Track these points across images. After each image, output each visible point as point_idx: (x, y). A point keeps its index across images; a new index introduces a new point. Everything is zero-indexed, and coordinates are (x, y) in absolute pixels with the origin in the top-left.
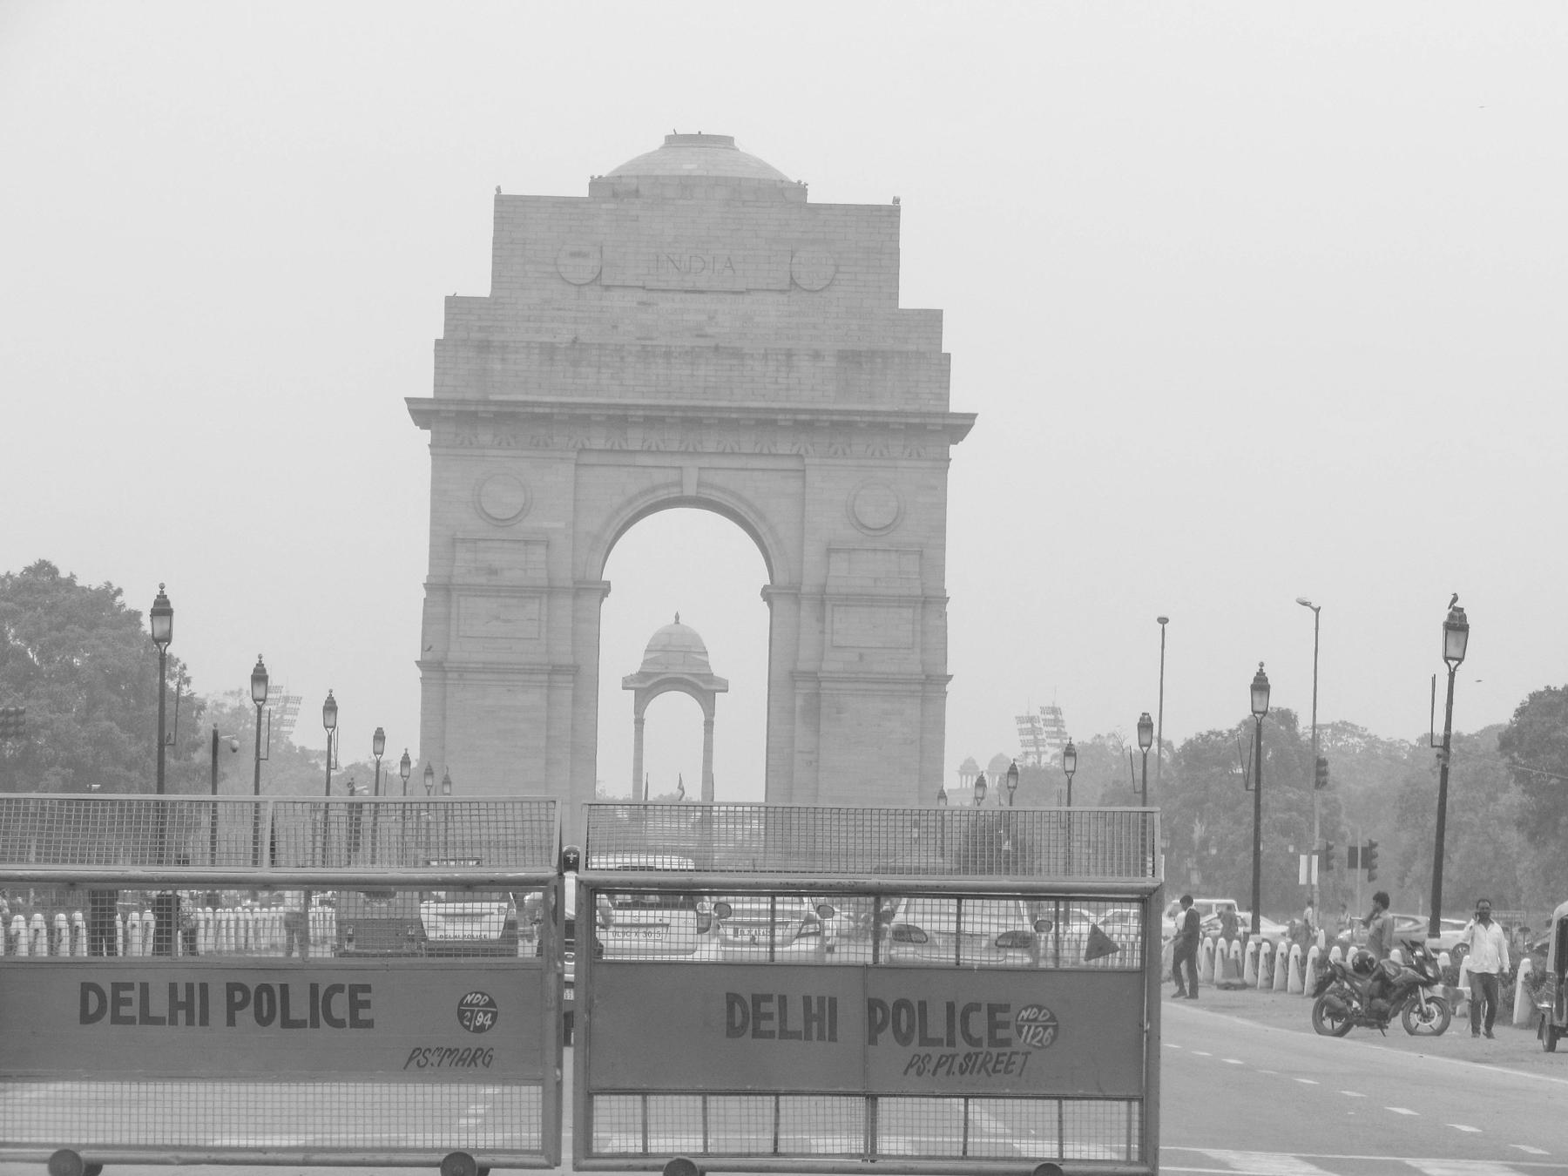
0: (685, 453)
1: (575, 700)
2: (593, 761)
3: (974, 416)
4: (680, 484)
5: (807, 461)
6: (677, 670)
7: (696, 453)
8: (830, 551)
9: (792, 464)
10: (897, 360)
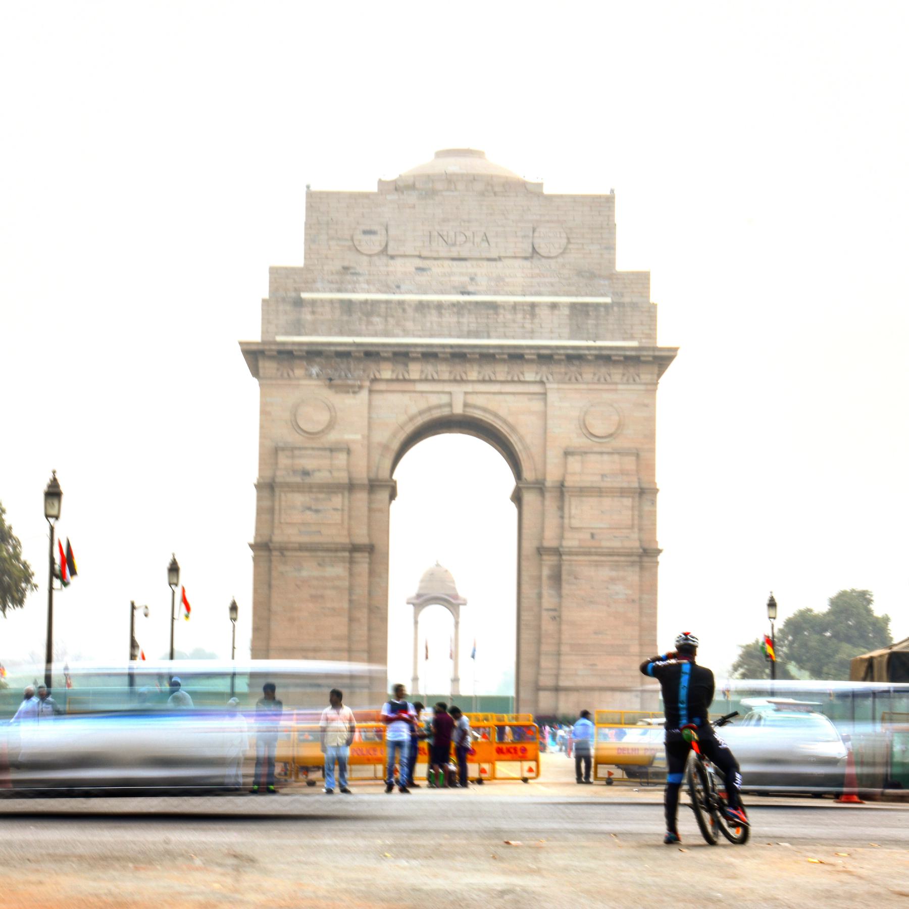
0: (455, 381)
1: (371, 573)
2: (384, 619)
3: (675, 350)
4: (450, 405)
5: (548, 386)
6: (438, 595)
7: (462, 381)
8: (567, 453)
9: (537, 388)
10: (616, 309)
